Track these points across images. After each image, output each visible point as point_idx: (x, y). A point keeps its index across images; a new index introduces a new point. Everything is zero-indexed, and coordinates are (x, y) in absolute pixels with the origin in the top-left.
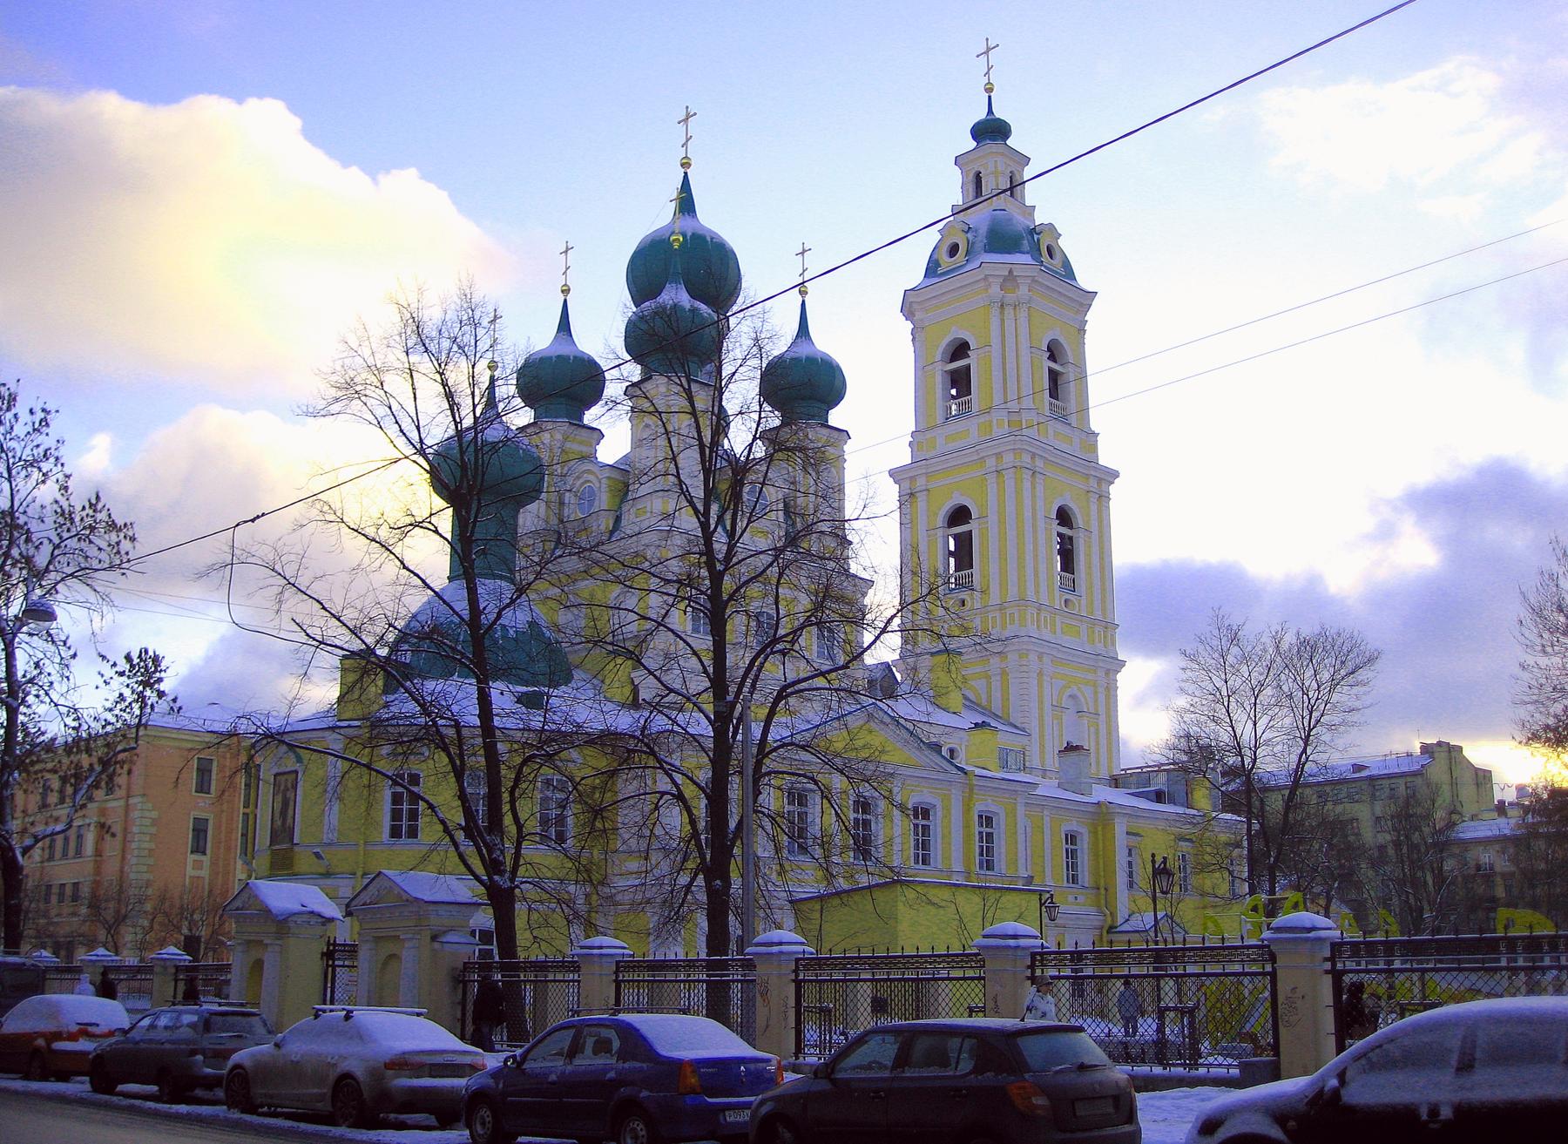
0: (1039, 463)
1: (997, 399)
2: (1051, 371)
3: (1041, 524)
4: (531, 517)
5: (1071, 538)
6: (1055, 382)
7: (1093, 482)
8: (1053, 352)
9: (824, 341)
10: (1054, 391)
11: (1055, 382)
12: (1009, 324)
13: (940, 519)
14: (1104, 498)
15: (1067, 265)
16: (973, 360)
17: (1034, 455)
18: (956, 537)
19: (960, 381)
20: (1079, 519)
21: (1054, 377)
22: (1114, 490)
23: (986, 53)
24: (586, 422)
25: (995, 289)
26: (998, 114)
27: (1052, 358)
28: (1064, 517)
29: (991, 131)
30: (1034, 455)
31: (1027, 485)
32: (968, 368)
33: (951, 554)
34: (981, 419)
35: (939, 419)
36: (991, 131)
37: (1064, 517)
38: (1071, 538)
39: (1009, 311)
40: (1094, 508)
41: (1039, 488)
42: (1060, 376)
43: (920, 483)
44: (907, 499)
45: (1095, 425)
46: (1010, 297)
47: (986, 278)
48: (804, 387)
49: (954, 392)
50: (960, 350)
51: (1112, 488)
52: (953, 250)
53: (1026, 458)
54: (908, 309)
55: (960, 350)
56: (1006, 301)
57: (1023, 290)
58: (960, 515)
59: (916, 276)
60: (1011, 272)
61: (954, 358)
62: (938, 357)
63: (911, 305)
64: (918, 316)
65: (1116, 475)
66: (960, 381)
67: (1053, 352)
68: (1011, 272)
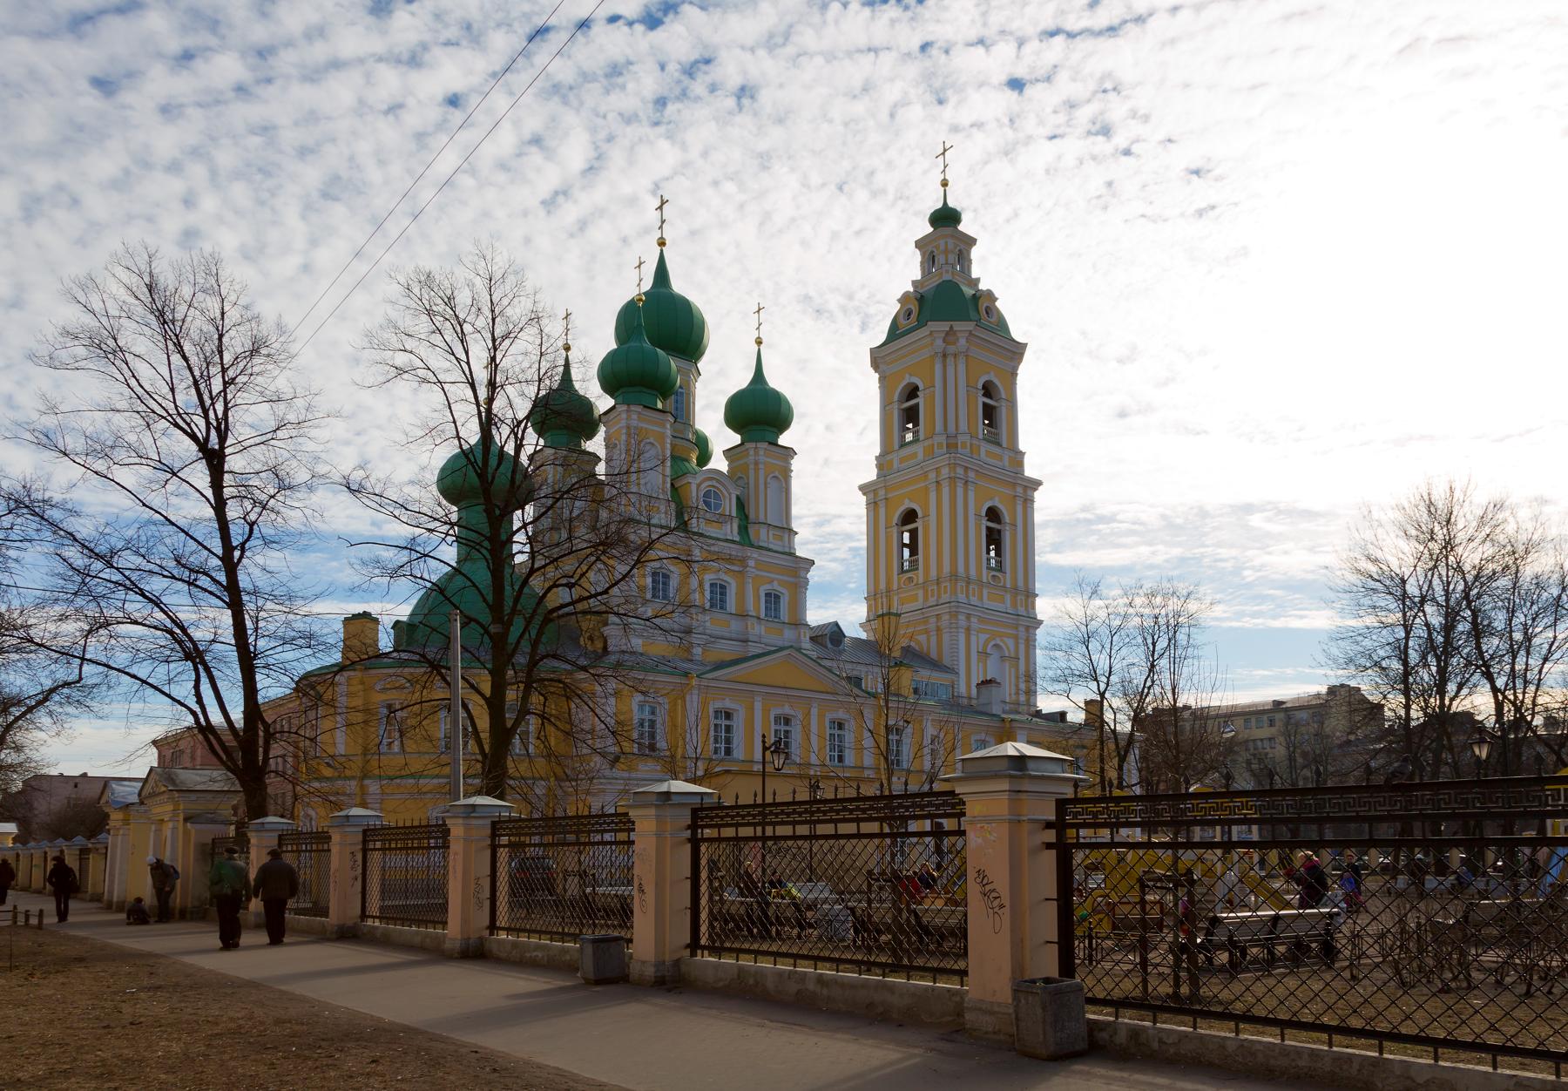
0: (971, 475)
1: (939, 427)
2: (985, 405)
5: (999, 531)
7: (1020, 490)
8: (988, 390)
11: (989, 412)
14: (1028, 502)
16: (920, 400)
17: (966, 468)
18: (909, 531)
19: (911, 415)
20: (1007, 518)
22: (1037, 495)
25: (939, 342)
26: (951, 204)
28: (993, 514)
29: (945, 218)
30: (966, 468)
31: (960, 491)
34: (927, 443)
35: (896, 446)
36: (945, 218)
37: (993, 514)
38: (999, 531)
39: (950, 360)
40: (1019, 509)
41: (971, 495)
42: (995, 408)
43: (882, 493)
44: (873, 506)
45: (1022, 446)
46: (951, 349)
48: (760, 413)
50: (913, 392)
51: (1036, 494)
53: (960, 471)
54: (875, 364)
57: (963, 341)
62: (896, 398)
63: (879, 358)
64: (882, 367)
65: (1039, 483)
66: (911, 415)
67: (988, 390)
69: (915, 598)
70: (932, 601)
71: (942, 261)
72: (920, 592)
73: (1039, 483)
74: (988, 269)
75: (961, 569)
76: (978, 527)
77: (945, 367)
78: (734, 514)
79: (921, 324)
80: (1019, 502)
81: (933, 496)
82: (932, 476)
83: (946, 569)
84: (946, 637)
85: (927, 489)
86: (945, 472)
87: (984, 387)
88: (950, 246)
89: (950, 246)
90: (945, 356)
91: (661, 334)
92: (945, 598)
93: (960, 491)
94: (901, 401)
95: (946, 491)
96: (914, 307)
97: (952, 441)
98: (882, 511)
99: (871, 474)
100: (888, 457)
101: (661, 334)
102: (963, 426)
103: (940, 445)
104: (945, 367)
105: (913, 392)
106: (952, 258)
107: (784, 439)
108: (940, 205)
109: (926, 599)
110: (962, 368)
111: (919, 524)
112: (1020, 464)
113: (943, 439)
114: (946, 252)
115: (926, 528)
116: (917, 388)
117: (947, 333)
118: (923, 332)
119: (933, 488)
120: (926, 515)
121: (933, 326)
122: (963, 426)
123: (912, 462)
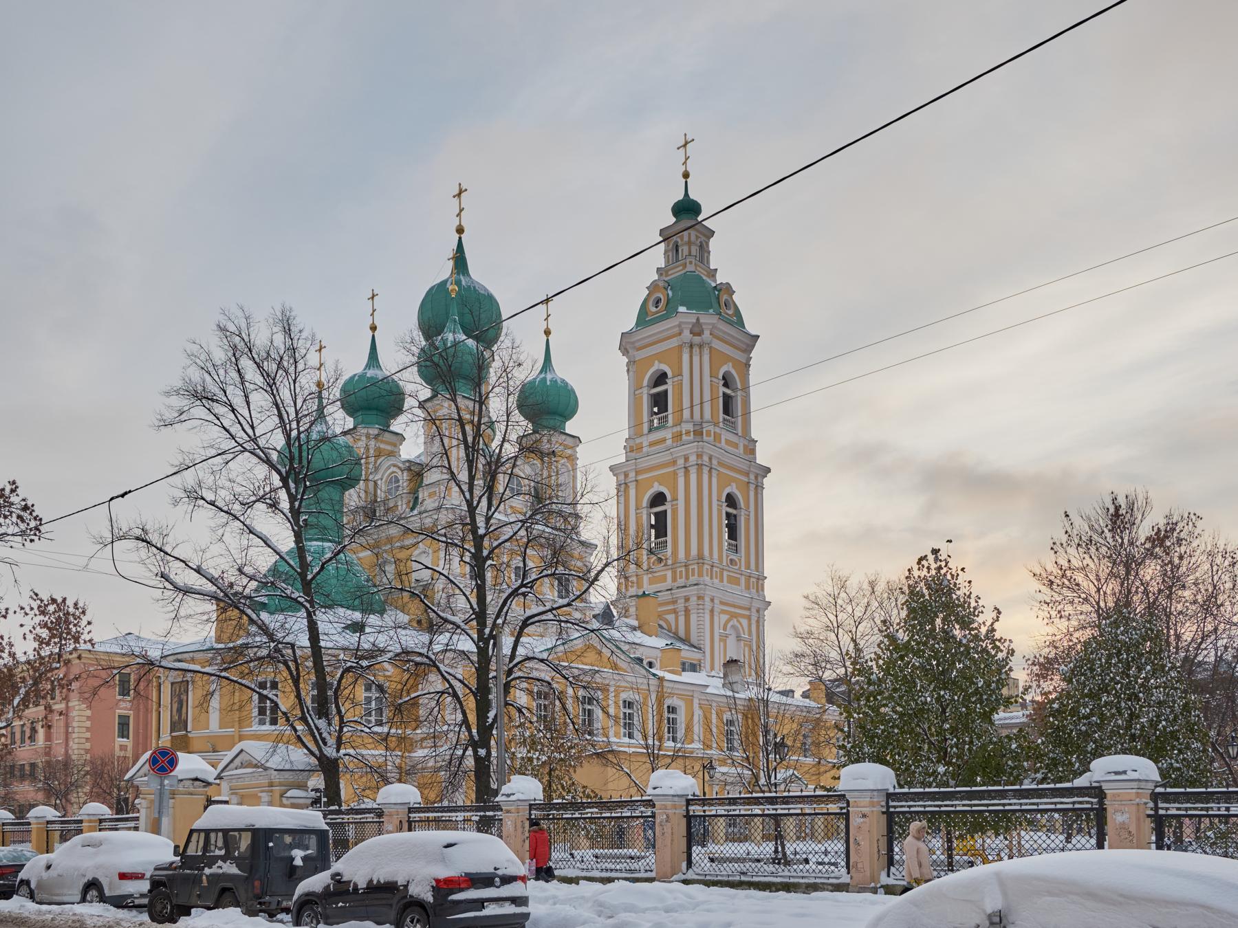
4: (353, 498)
5: (735, 516)
6: (728, 403)
9: (562, 371)
10: (727, 411)
11: (728, 403)
12: (696, 359)
15: (737, 313)
16: (669, 387)
18: (656, 514)
19: (660, 402)
20: (742, 504)
21: (727, 400)
22: (767, 481)
23: (685, 146)
24: (392, 428)
27: (726, 385)
28: (731, 501)
29: (686, 209)
31: (705, 477)
32: (666, 392)
33: (652, 526)
34: (675, 430)
35: (646, 429)
36: (686, 209)
37: (731, 501)
39: (696, 350)
41: (714, 480)
46: (697, 339)
47: (679, 326)
49: (656, 410)
50: (661, 378)
52: (658, 301)
54: (624, 349)
55: (661, 378)
58: (659, 499)
59: (630, 323)
61: (656, 384)
62: (645, 383)
63: (627, 344)
65: (768, 470)
66: (660, 402)
69: (664, 579)
70: (681, 582)
71: (686, 252)
72: (669, 574)
73: (768, 470)
74: (726, 261)
75: (706, 553)
76: (720, 511)
81: (681, 481)
83: (694, 552)
84: (693, 618)
85: (675, 473)
86: (693, 459)
87: (724, 378)
88: (693, 238)
89: (693, 238)
90: (691, 346)
91: (460, 324)
92: (693, 579)
93: (705, 477)
101: (460, 324)
102: (707, 416)
103: (688, 433)
106: (694, 250)
107: (571, 427)
109: (674, 580)
110: (706, 358)
111: (667, 507)
112: (753, 452)
113: (690, 427)
114: (689, 243)
115: (675, 512)
119: (681, 473)
120: (675, 499)
122: (707, 416)
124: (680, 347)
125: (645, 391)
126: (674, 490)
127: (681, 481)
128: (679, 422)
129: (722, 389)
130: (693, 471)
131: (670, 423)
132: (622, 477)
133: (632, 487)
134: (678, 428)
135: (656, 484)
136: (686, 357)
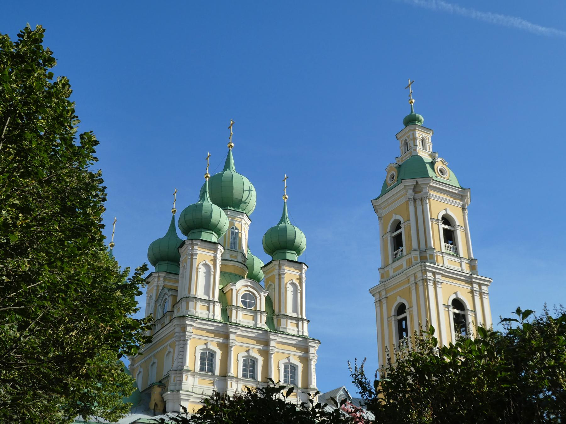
3: (442, 309)
7: (476, 286)
13: (393, 312)
19: (398, 242)
20: (469, 306)
35: (390, 262)
39: (419, 203)
43: (383, 293)
50: (397, 225)
56: (417, 198)
60: (417, 182)
62: (389, 230)
64: (380, 211)
66: (398, 242)
68: (417, 182)
77: (415, 207)
78: (263, 309)
79: (399, 182)
80: (476, 294)
81: (414, 292)
82: (412, 279)
85: (410, 288)
90: (415, 200)
94: (392, 232)
95: (421, 288)
96: (395, 173)
97: (424, 254)
98: (385, 306)
99: (375, 280)
100: (386, 269)
103: (416, 258)
104: (415, 207)
105: (397, 225)
108: (409, 113)
113: (417, 254)
116: (400, 223)
117: (415, 187)
118: (401, 186)
119: (413, 287)
120: (411, 307)
121: (405, 183)
123: (401, 270)
124: (407, 202)
125: (389, 235)
126: (410, 302)
127: (414, 292)
128: (410, 250)
129: (443, 226)
130: (420, 284)
131: (405, 253)
132: (377, 296)
133: (384, 301)
134: (409, 256)
135: (398, 298)
136: (411, 208)
